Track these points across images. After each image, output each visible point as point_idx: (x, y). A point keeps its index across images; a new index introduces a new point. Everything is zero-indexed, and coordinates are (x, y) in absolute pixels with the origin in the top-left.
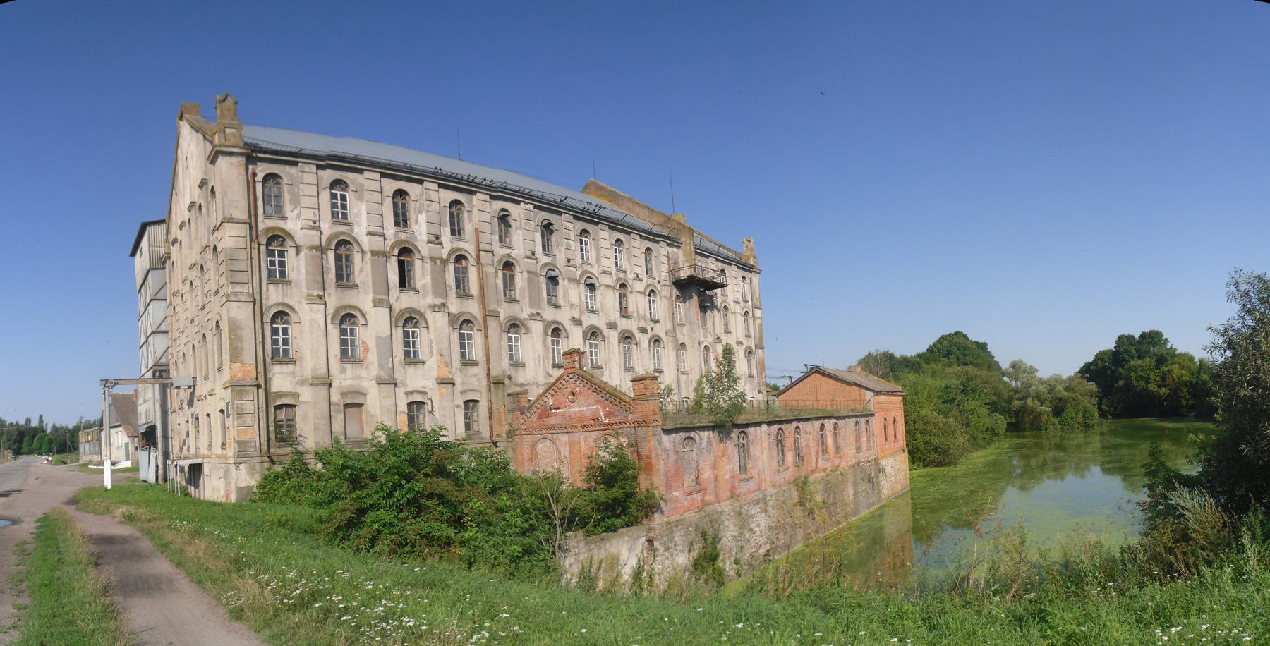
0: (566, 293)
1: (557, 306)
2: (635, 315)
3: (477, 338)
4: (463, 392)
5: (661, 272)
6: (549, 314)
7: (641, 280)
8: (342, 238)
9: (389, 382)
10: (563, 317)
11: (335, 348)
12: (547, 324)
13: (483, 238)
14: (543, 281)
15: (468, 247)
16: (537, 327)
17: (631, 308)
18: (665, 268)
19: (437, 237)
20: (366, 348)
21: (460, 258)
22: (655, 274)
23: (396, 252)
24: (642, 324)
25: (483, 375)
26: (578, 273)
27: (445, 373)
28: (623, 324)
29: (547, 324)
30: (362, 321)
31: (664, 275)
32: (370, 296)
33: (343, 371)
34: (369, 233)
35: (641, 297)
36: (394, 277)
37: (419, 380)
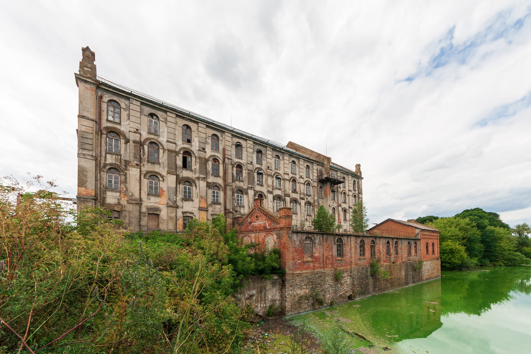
0: (267, 180)
1: (262, 185)
2: (299, 192)
3: (222, 194)
4: (212, 215)
5: (314, 176)
6: (258, 188)
7: (303, 178)
8: (153, 141)
10: (264, 190)
11: (145, 189)
12: (256, 192)
13: (227, 152)
14: (256, 174)
15: (220, 156)
16: (251, 193)
17: (298, 189)
18: (316, 174)
19: (204, 149)
21: (215, 160)
22: (311, 176)
23: (182, 152)
24: (302, 196)
25: (223, 209)
26: (273, 173)
27: (204, 205)
28: (294, 195)
30: (161, 179)
31: (315, 178)
32: (166, 169)
33: (149, 199)
34: (168, 141)
35: (302, 186)
36: (180, 162)
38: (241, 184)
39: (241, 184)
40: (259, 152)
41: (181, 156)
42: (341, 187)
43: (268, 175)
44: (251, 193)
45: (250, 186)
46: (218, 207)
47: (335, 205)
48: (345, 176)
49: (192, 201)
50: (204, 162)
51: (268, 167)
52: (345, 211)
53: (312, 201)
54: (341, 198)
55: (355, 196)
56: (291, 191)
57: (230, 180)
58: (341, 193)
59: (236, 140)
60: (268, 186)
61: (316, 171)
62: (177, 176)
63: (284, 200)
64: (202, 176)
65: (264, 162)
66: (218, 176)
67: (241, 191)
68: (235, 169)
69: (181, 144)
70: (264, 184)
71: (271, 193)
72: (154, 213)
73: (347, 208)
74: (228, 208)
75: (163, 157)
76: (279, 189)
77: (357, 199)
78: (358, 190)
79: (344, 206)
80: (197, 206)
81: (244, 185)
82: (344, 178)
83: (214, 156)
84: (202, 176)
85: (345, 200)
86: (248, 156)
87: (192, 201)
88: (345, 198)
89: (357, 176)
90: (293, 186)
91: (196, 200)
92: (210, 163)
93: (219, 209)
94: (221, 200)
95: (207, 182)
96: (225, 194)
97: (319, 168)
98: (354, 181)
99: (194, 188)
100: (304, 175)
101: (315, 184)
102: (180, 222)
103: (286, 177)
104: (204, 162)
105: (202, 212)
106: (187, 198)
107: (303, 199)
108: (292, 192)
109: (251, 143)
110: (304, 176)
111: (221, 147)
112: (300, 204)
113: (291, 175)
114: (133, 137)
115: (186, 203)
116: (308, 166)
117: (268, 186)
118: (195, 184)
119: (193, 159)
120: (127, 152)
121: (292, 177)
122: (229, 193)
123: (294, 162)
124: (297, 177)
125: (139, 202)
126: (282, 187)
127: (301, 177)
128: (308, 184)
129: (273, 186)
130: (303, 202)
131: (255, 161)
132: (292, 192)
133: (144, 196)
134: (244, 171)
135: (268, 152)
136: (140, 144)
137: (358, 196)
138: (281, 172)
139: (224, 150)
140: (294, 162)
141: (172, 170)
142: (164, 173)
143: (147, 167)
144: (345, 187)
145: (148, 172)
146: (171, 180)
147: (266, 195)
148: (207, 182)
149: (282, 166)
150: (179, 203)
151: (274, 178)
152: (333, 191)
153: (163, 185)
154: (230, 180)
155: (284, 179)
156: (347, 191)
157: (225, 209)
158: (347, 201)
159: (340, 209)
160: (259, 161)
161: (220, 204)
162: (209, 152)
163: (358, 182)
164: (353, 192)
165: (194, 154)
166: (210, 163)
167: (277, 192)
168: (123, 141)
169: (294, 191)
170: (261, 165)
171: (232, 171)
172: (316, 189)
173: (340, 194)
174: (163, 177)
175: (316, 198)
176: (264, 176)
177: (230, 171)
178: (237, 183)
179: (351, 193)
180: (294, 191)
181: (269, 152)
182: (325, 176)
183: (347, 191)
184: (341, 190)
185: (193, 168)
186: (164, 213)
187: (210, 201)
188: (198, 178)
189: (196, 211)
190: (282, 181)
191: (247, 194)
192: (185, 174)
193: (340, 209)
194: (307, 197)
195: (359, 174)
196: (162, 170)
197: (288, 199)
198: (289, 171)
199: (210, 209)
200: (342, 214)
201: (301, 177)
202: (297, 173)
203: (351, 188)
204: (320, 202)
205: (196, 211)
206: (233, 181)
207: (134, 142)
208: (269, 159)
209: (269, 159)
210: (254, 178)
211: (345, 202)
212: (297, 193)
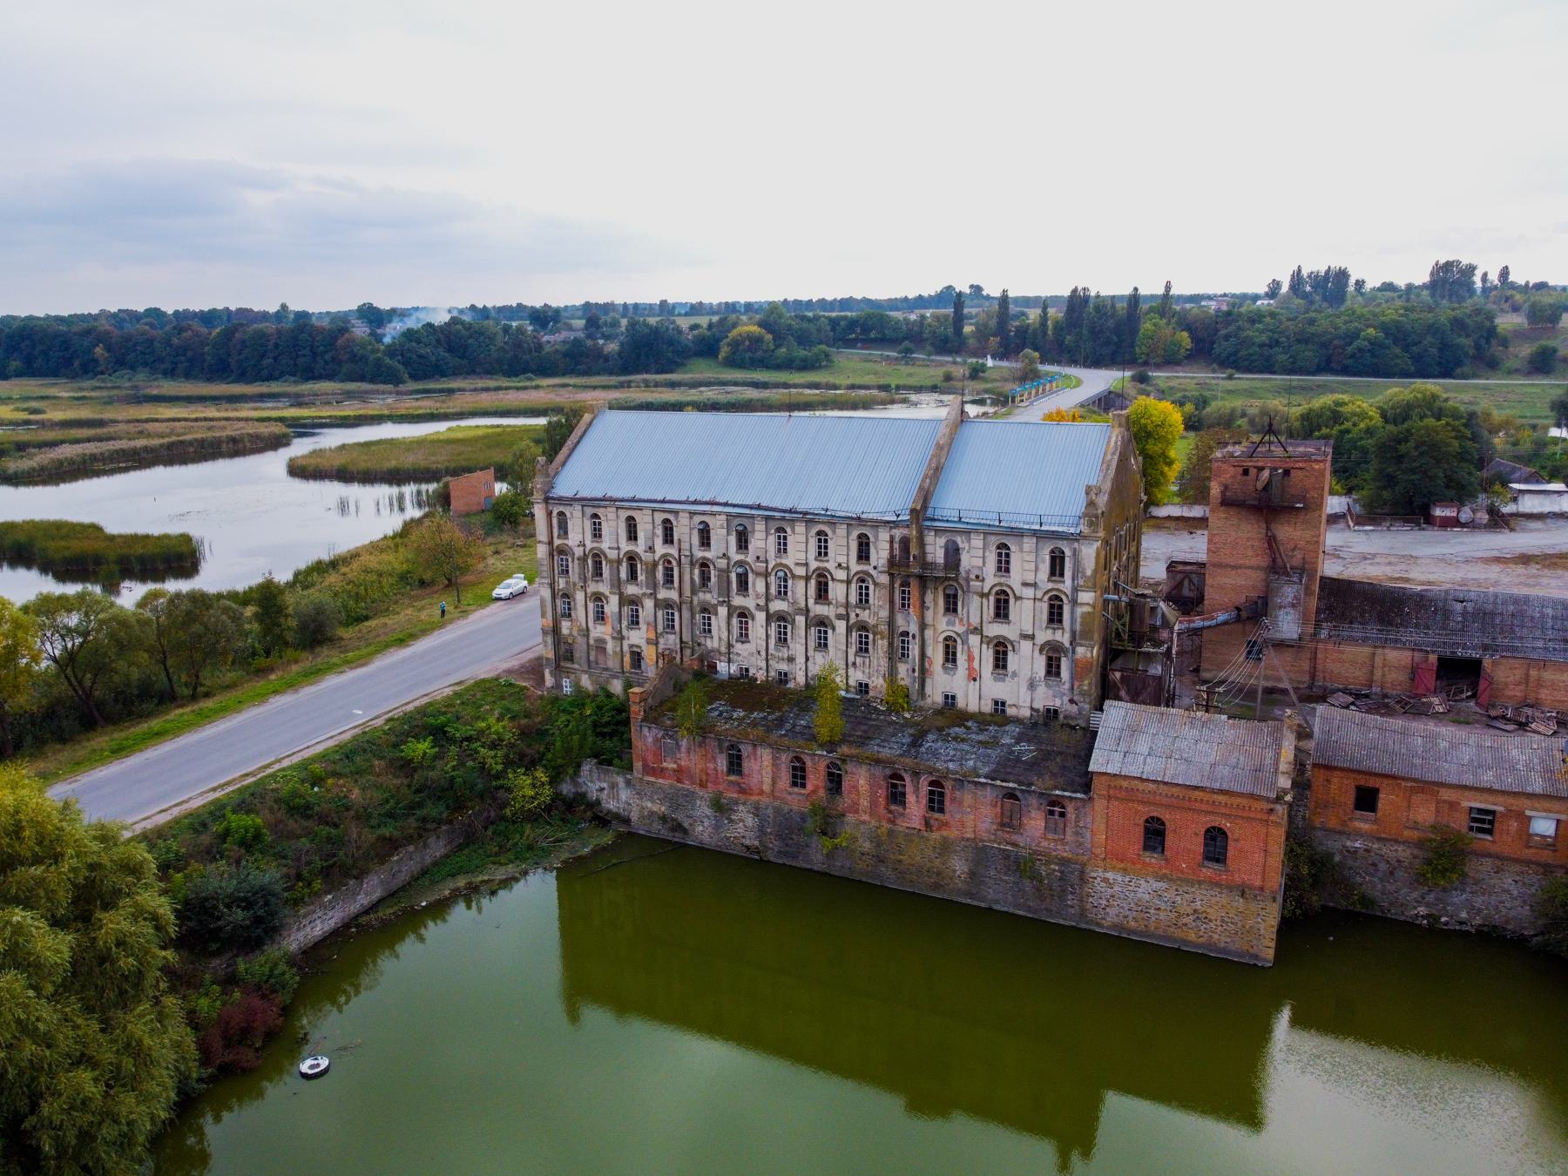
9: (620, 638)
11: (591, 615)
15: (673, 551)
36: (623, 575)
37: (637, 637)
38: (708, 597)
39: (708, 597)
57: (687, 592)
62: (621, 595)
67: (706, 609)
69: (626, 547)
72: (600, 646)
81: (709, 597)
92: (660, 568)
93: (671, 640)
102: (627, 659)
115: (632, 633)
125: (586, 633)
133: (591, 624)
136: (584, 559)
141: (617, 585)
143: (593, 587)
145: (594, 594)
150: (625, 632)
154: (687, 592)
166: (660, 568)
186: (610, 646)
189: (643, 643)
192: (631, 590)
196: (604, 588)
199: (661, 641)
205: (643, 643)
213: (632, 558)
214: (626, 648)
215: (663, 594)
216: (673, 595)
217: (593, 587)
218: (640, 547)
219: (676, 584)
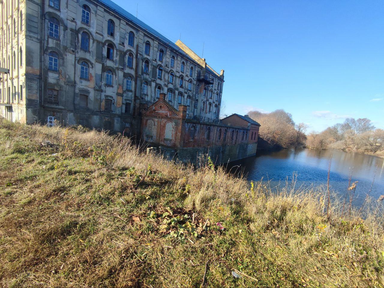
0: (164, 76)
1: (161, 79)
3: (133, 83)
4: (126, 100)
5: (195, 76)
6: (158, 81)
7: (188, 77)
10: (162, 83)
12: (157, 84)
13: (139, 49)
14: (158, 70)
15: (134, 51)
16: (153, 84)
17: (184, 85)
18: (196, 75)
19: (123, 44)
20: (92, 76)
24: (186, 91)
25: (133, 96)
26: (169, 70)
27: (121, 91)
29: (157, 84)
30: (90, 66)
31: (195, 77)
32: (95, 58)
34: (97, 33)
35: (187, 82)
36: (105, 53)
37: (110, 92)
40: (162, 51)
41: (106, 47)
42: (211, 86)
43: (167, 72)
44: (153, 84)
45: (153, 79)
46: (130, 94)
47: (205, 99)
48: (214, 78)
49: (112, 87)
50: (123, 54)
51: (167, 65)
52: (210, 104)
53: (191, 95)
54: (209, 94)
55: (217, 94)
56: (179, 86)
57: (140, 73)
58: (210, 91)
59: (147, 39)
60: (165, 81)
61: (197, 72)
63: (174, 93)
64: (121, 67)
65: (164, 60)
66: (132, 68)
68: (144, 63)
70: (162, 78)
71: (166, 86)
73: (212, 103)
74: (137, 95)
75: (93, 46)
76: (172, 84)
77: (218, 96)
78: (220, 90)
79: (211, 101)
80: (116, 91)
81: (148, 77)
82: (213, 80)
83: (130, 50)
84: (121, 67)
85: (211, 97)
86: (154, 54)
87: (112, 87)
88: (212, 95)
89: (221, 79)
90: (181, 82)
91: (116, 87)
94: (133, 89)
95: (124, 73)
96: (136, 84)
97: (199, 69)
98: (219, 82)
99: (114, 76)
100: (189, 74)
101: (195, 82)
103: (178, 75)
104: (123, 54)
105: (119, 97)
106: (109, 85)
107: (186, 93)
108: (180, 87)
109: (157, 43)
110: (189, 76)
111: (135, 44)
112: (184, 97)
113: (181, 73)
114: (70, 25)
116: (192, 67)
117: (165, 81)
118: (116, 74)
119: (115, 51)
120: (65, 38)
121: (181, 75)
122: (139, 83)
123: (183, 63)
124: (184, 75)
126: (174, 82)
127: (187, 76)
128: (191, 82)
129: (168, 81)
130: (186, 95)
131: (158, 59)
132: (180, 87)
134: (150, 66)
135: (168, 53)
136: (75, 32)
137: (220, 94)
138: (174, 70)
139: (137, 46)
140: (183, 63)
142: (93, 61)
143: (81, 54)
144: (212, 87)
146: (98, 67)
147: (163, 87)
148: (124, 73)
149: (175, 65)
150: (103, 88)
151: (170, 75)
152: (205, 89)
153: (92, 71)
155: (176, 76)
156: (214, 90)
157: (135, 96)
158: (212, 98)
159: (208, 102)
160: (161, 59)
161: (131, 91)
162: (127, 47)
163: (221, 83)
164: (217, 91)
165: (116, 47)
167: (171, 86)
168: (62, 28)
169: (181, 86)
170: (162, 62)
171: (142, 65)
172: (195, 86)
173: (209, 91)
174: (92, 64)
175: (194, 93)
176: (163, 71)
177: (140, 65)
178: (145, 75)
179: (215, 92)
180: (181, 86)
181: (168, 53)
182: (202, 77)
183: (214, 90)
184: (210, 88)
185: (114, 59)
187: (125, 89)
188: (118, 69)
189: (114, 95)
190: (174, 78)
191: (150, 85)
192: (109, 63)
193: (208, 102)
194: (189, 92)
195: (222, 78)
196: (91, 58)
197: (177, 92)
198: (179, 69)
199: (125, 95)
200: (208, 106)
201: (187, 76)
202: (185, 71)
203: (216, 88)
204: (197, 97)
206: (142, 74)
207: (72, 30)
208: (167, 58)
209: (167, 58)
210: (156, 73)
211: (211, 98)
212: (183, 88)
213: (111, 46)
214: (103, 97)
215: (127, 70)
216: (133, 73)
217: (81, 54)
218: (116, 41)
219: (134, 67)
